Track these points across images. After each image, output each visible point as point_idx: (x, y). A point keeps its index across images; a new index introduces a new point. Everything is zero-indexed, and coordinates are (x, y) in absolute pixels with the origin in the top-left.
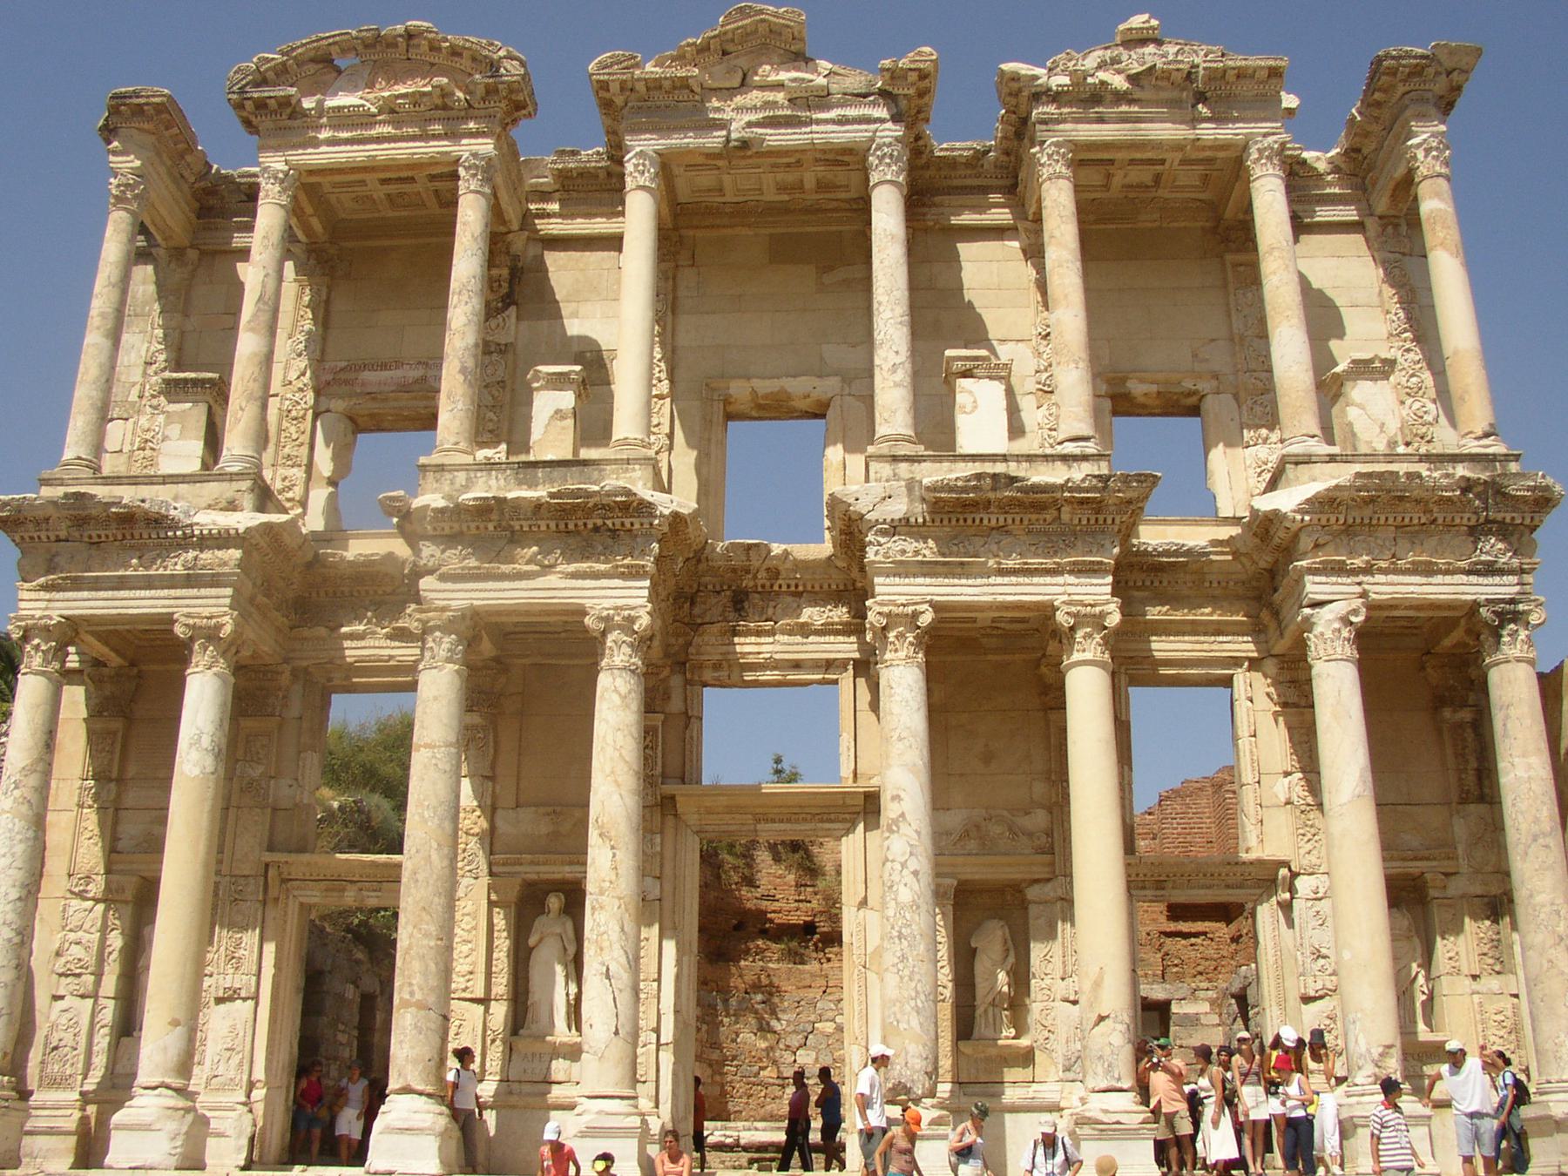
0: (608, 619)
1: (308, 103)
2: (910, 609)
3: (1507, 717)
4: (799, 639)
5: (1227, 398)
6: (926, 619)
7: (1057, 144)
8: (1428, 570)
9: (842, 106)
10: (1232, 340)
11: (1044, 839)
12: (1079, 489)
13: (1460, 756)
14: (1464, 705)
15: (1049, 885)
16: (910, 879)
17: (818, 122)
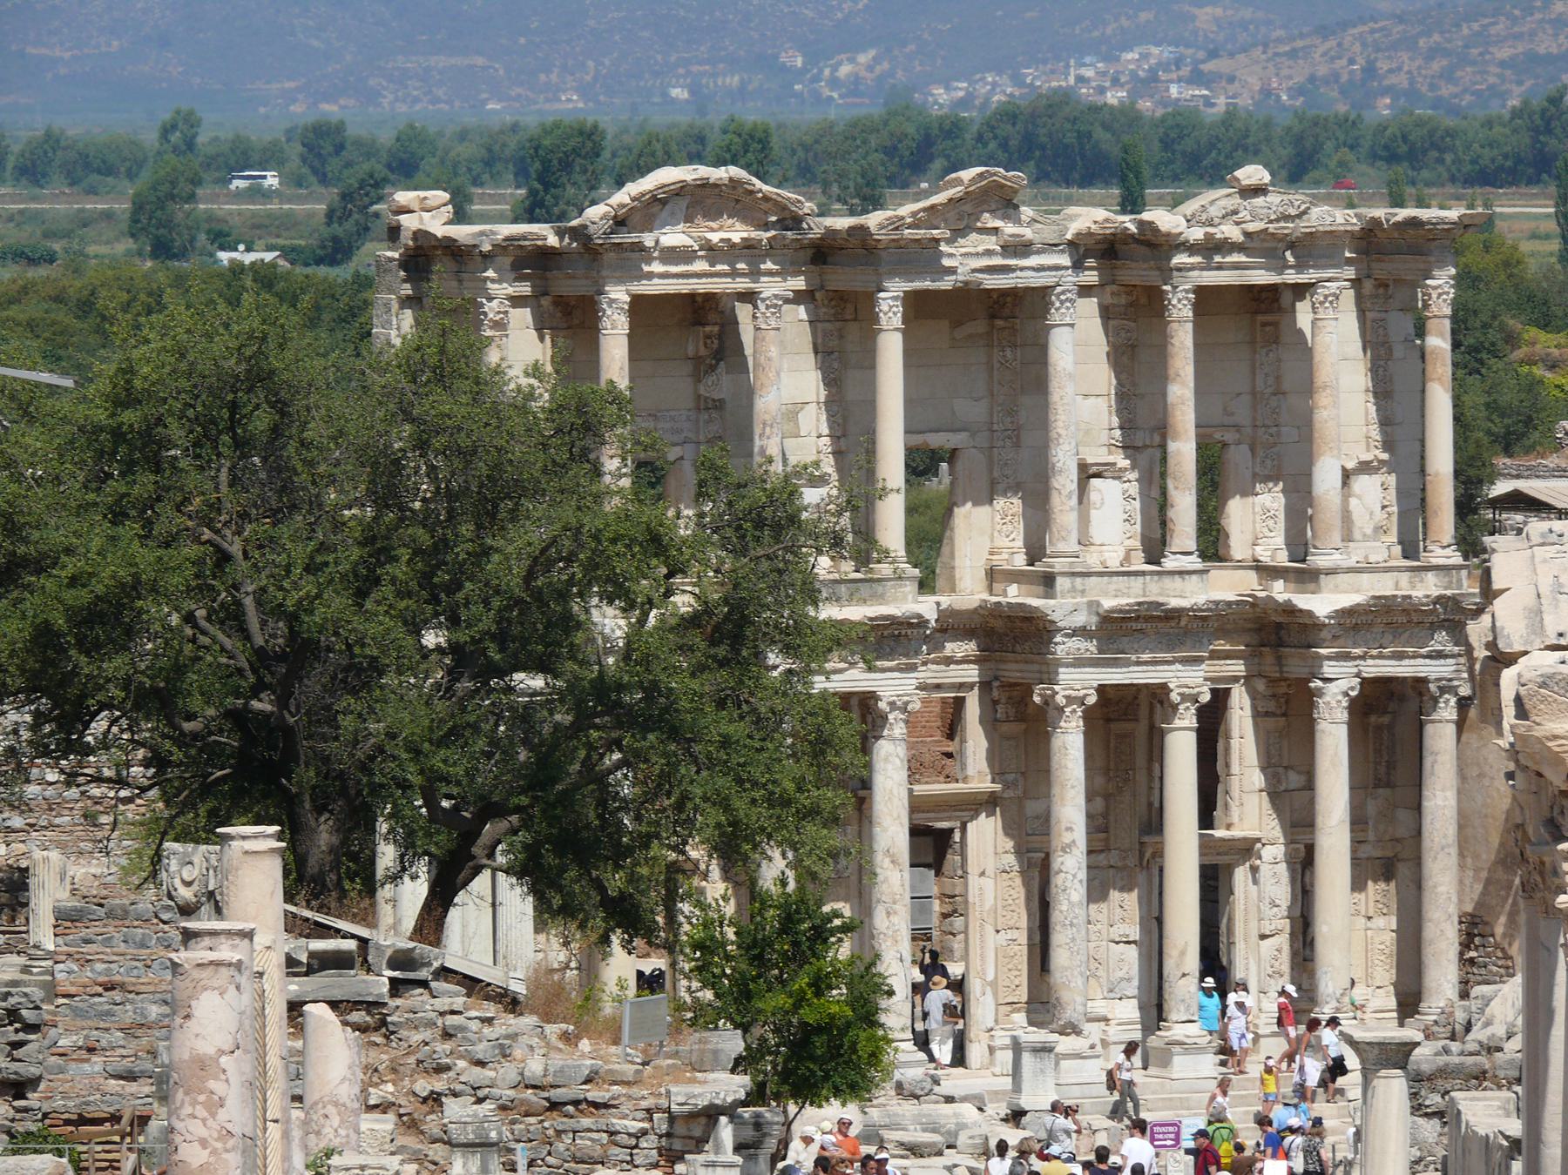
0: (892, 704)
1: (648, 240)
2: (1082, 692)
3: (1435, 761)
4: (943, 667)
5: (1244, 448)
6: (1092, 700)
7: (1187, 291)
8: (1400, 656)
9: (1039, 252)
10: (1254, 393)
11: (1101, 820)
12: (1201, 610)
13: (1378, 751)
14: (1385, 712)
15: (1102, 856)
16: (1078, 886)
17: (1022, 269)
